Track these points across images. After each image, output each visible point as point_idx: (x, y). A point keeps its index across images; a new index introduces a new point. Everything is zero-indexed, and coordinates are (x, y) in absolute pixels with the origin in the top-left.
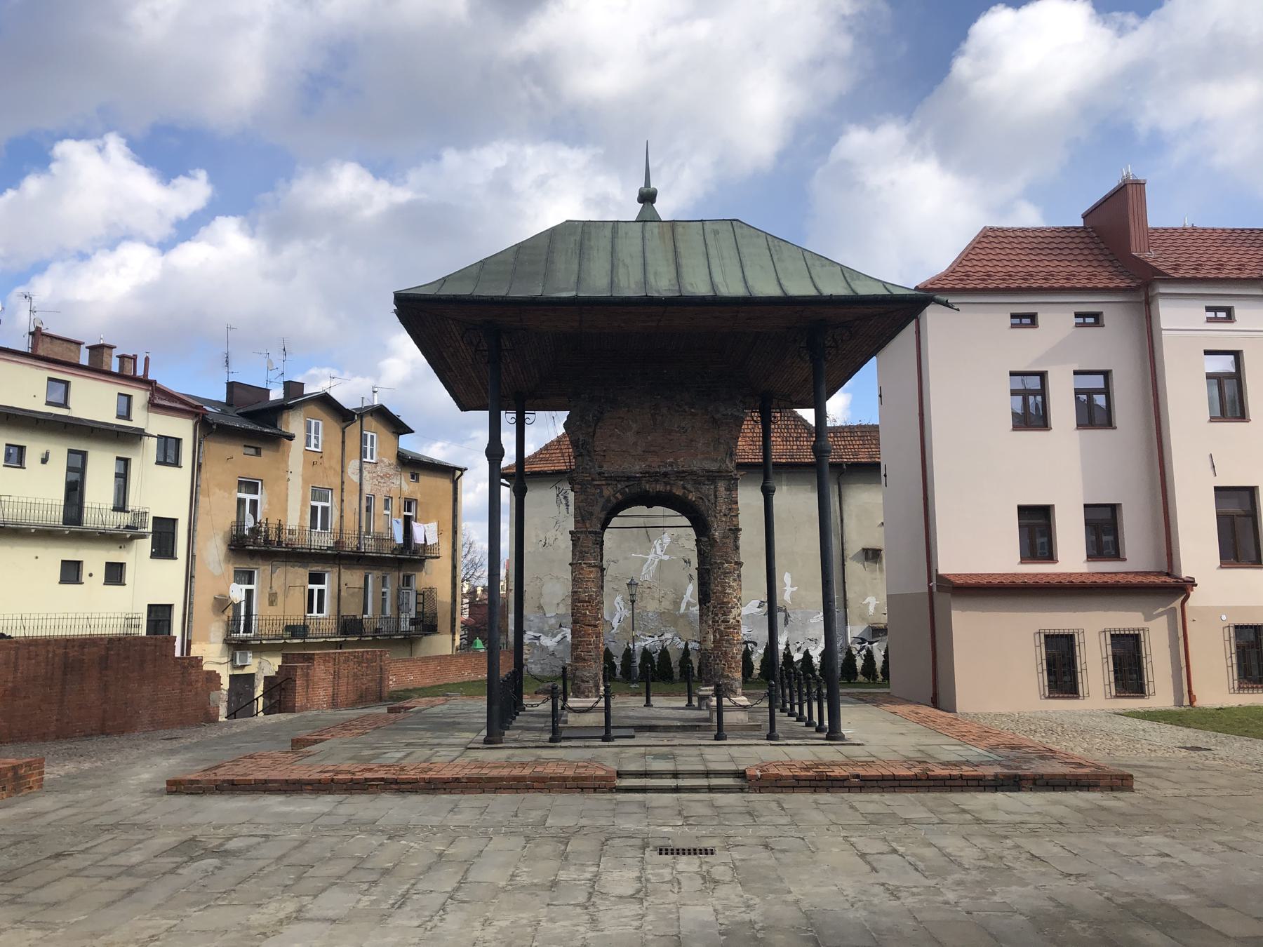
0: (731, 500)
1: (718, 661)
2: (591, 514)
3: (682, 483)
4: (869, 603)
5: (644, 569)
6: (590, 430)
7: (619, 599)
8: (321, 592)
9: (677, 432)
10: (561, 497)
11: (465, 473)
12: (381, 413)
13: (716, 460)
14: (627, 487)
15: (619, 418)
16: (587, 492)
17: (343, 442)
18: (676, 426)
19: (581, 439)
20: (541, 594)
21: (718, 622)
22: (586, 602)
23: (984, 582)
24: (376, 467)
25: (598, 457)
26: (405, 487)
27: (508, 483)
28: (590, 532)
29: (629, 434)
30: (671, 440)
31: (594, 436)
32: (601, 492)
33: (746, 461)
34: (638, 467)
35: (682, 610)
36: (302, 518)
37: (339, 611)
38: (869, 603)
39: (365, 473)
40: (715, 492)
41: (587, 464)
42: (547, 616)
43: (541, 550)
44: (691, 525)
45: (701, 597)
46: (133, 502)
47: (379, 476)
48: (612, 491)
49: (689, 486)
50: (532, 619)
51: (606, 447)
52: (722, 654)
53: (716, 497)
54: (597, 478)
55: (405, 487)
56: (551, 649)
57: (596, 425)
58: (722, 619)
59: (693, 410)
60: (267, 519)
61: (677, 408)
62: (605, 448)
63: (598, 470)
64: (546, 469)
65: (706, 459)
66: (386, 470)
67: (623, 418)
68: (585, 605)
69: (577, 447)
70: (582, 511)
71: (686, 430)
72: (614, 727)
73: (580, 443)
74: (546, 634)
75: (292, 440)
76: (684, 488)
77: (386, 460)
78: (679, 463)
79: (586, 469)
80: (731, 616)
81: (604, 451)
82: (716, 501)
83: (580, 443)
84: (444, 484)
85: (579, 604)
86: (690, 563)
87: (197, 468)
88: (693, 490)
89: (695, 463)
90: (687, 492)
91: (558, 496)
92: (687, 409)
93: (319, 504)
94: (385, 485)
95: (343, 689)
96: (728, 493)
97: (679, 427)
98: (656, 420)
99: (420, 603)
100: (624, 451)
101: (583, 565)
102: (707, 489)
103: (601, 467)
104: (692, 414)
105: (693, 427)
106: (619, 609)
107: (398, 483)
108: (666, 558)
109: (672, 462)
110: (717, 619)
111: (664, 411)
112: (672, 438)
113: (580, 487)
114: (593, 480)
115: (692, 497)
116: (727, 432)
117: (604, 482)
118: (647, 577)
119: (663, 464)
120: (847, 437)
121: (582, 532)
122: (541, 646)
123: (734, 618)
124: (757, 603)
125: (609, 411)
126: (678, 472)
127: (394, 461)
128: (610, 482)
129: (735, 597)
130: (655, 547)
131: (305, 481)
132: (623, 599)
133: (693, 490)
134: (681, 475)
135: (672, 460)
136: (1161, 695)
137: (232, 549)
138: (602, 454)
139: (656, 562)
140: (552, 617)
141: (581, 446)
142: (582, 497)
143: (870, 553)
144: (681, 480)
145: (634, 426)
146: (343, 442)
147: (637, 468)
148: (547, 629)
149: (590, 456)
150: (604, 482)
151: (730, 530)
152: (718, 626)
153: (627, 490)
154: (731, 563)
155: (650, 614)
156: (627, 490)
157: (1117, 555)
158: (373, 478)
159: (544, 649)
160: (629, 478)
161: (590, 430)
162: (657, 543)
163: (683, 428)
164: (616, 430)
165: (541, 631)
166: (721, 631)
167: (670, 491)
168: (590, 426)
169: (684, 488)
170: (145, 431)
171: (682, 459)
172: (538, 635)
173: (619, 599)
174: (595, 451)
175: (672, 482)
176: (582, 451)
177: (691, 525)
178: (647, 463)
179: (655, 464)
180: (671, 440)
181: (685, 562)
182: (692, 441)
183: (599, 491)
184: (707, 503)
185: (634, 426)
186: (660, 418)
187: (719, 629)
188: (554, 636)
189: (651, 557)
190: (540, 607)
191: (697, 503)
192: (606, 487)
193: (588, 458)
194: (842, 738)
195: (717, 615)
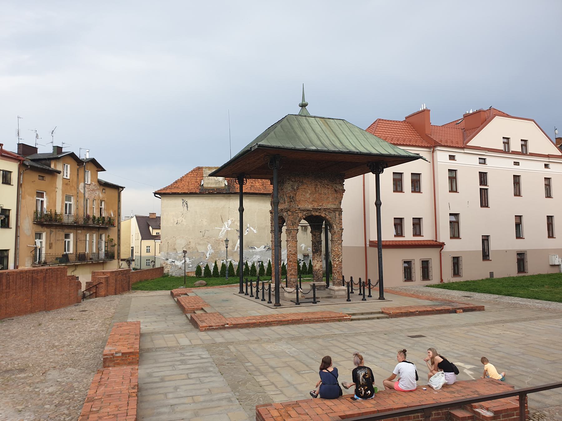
1: (336, 274)
2: (295, 223)
5: (220, 233)
6: (295, 193)
7: (209, 245)
10: (185, 204)
11: (124, 189)
12: (93, 161)
13: (335, 205)
15: (304, 188)
17: (78, 175)
20: (175, 244)
22: (294, 254)
23: (391, 243)
24: (90, 186)
26: (101, 195)
27: (160, 197)
28: (295, 230)
29: (307, 194)
33: (261, 192)
34: (310, 206)
35: (235, 250)
36: (62, 209)
37: (76, 251)
39: (86, 189)
42: (178, 252)
43: (175, 225)
45: (314, 251)
49: (327, 214)
50: (171, 254)
53: (335, 218)
55: (101, 195)
56: (180, 266)
60: (51, 210)
64: (178, 191)
65: (333, 204)
66: (93, 187)
72: (312, 298)
73: (291, 197)
74: (177, 260)
75: (60, 174)
76: (325, 214)
77: (93, 183)
80: (340, 259)
83: (291, 197)
84: (114, 193)
87: (19, 185)
91: (183, 203)
93: (68, 203)
95: (118, 286)
102: (332, 214)
103: (298, 206)
104: (328, 188)
105: (328, 193)
106: (209, 250)
107: (98, 193)
108: (229, 229)
110: (335, 260)
111: (319, 186)
114: (296, 211)
115: (327, 217)
118: (221, 237)
122: (175, 265)
124: (264, 246)
127: (97, 184)
130: (225, 225)
131: (63, 192)
132: (211, 245)
134: (325, 210)
135: (321, 204)
136: (435, 279)
137: (35, 224)
139: (225, 231)
140: (180, 253)
142: (292, 217)
143: (303, 228)
147: (310, 207)
148: (178, 258)
154: (340, 240)
155: (222, 252)
157: (420, 235)
158: (89, 191)
159: (176, 266)
160: (308, 210)
162: (226, 223)
165: (175, 259)
167: (321, 215)
169: (325, 214)
172: (174, 261)
173: (209, 245)
179: (316, 206)
182: (328, 198)
188: (181, 261)
189: (223, 229)
190: (175, 249)
194: (384, 299)
195: (335, 258)
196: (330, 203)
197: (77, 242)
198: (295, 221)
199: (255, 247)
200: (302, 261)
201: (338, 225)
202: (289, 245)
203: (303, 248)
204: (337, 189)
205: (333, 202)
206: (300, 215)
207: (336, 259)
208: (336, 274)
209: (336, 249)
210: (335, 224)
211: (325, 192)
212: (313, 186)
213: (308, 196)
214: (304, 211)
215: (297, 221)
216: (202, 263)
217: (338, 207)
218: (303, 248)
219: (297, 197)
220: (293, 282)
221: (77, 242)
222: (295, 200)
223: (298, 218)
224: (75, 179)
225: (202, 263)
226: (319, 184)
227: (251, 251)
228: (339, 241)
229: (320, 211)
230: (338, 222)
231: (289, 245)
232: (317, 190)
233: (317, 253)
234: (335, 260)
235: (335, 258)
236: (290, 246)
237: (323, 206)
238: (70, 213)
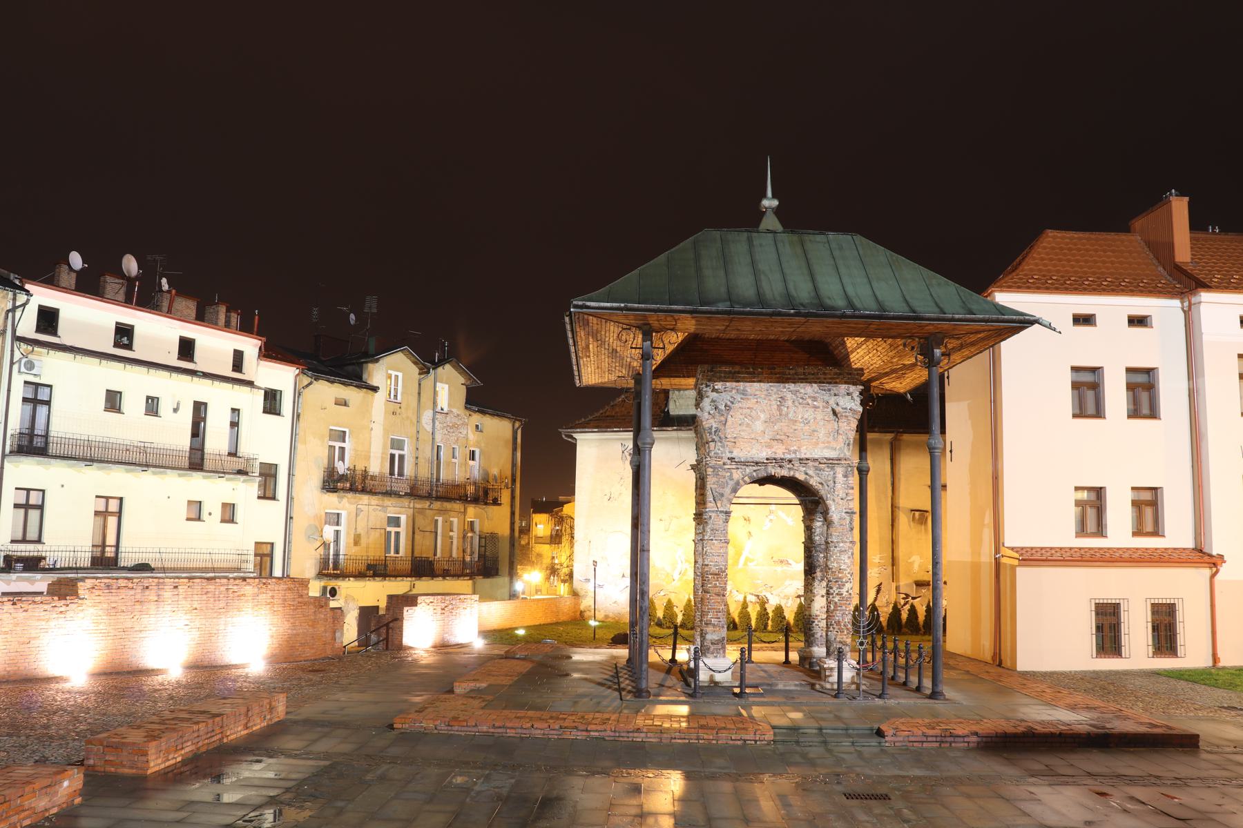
0: (848, 486)
2: (722, 495)
3: (804, 469)
4: (914, 561)
8: (397, 534)
9: (800, 423)
13: (835, 449)
14: (755, 471)
16: (719, 475)
17: (419, 394)
18: (800, 417)
21: (832, 594)
22: (716, 574)
25: (728, 443)
28: (721, 512)
29: (757, 423)
30: (795, 430)
31: (725, 424)
32: (731, 473)
38: (914, 561)
39: (437, 423)
40: (835, 478)
41: (719, 449)
44: (798, 503)
45: (807, 568)
46: (244, 450)
47: (448, 426)
48: (741, 475)
49: (810, 472)
52: (835, 622)
54: (729, 462)
57: (728, 414)
58: (837, 592)
59: (815, 403)
60: (355, 466)
61: (801, 401)
62: (735, 436)
63: (729, 455)
66: (455, 420)
67: (752, 408)
68: (715, 577)
70: (714, 492)
71: (809, 421)
73: (714, 430)
75: (377, 392)
76: (807, 474)
78: (802, 451)
79: (718, 454)
81: (735, 438)
82: (834, 486)
83: (714, 430)
85: (710, 577)
86: (749, 520)
87: (297, 417)
88: (814, 475)
89: (816, 451)
90: (808, 477)
91: (623, 452)
92: (810, 402)
93: (397, 453)
94: (454, 434)
96: (845, 479)
97: (801, 419)
98: (782, 410)
99: (482, 547)
100: (752, 439)
101: (714, 541)
104: (816, 407)
105: (815, 418)
107: (465, 432)
109: (796, 451)
112: (796, 427)
113: (712, 470)
114: (724, 464)
116: (845, 424)
117: (734, 467)
119: (787, 451)
121: (713, 511)
123: (847, 592)
125: (739, 402)
126: (800, 459)
128: (739, 466)
129: (849, 573)
133: (814, 475)
135: (795, 448)
138: (733, 441)
141: (713, 433)
144: (804, 467)
145: (762, 416)
146: (419, 394)
147: (762, 454)
149: (721, 442)
150: (734, 467)
151: (846, 513)
152: (833, 597)
153: (755, 474)
154: (846, 542)
156: (755, 474)
157: (1157, 532)
161: (723, 419)
163: (806, 419)
164: (746, 419)
166: (836, 603)
168: (723, 415)
169: (807, 474)
170: (255, 383)
171: (805, 447)
174: (726, 438)
175: (795, 468)
176: (714, 437)
177: (798, 503)
178: (773, 450)
179: (780, 451)
180: (795, 430)
181: (745, 519)
182: (814, 431)
183: (729, 474)
184: (826, 487)
185: (762, 416)
186: (786, 409)
187: (833, 601)
191: (816, 487)
192: (735, 470)
193: (719, 444)
195: (831, 588)
196: (821, 445)
197: (414, 533)
198: (721, 491)
199: (790, 561)
201: (841, 502)
203: (916, 566)
204: (838, 409)
205: (828, 442)
206: (737, 475)
207: (835, 589)
208: (831, 629)
210: (834, 500)
211: (806, 416)
212: (774, 402)
213: (759, 426)
214: (746, 463)
215: (727, 490)
216: (662, 593)
217: (842, 456)
218: (916, 566)
219: (728, 431)
220: (712, 643)
221: (414, 533)
222: (722, 436)
223: (731, 483)
224: (414, 403)
225: (662, 593)
226: (789, 396)
227: (779, 568)
228: (841, 545)
229: (790, 466)
230: (842, 494)
232: (784, 413)
237: (800, 453)
238: (401, 474)
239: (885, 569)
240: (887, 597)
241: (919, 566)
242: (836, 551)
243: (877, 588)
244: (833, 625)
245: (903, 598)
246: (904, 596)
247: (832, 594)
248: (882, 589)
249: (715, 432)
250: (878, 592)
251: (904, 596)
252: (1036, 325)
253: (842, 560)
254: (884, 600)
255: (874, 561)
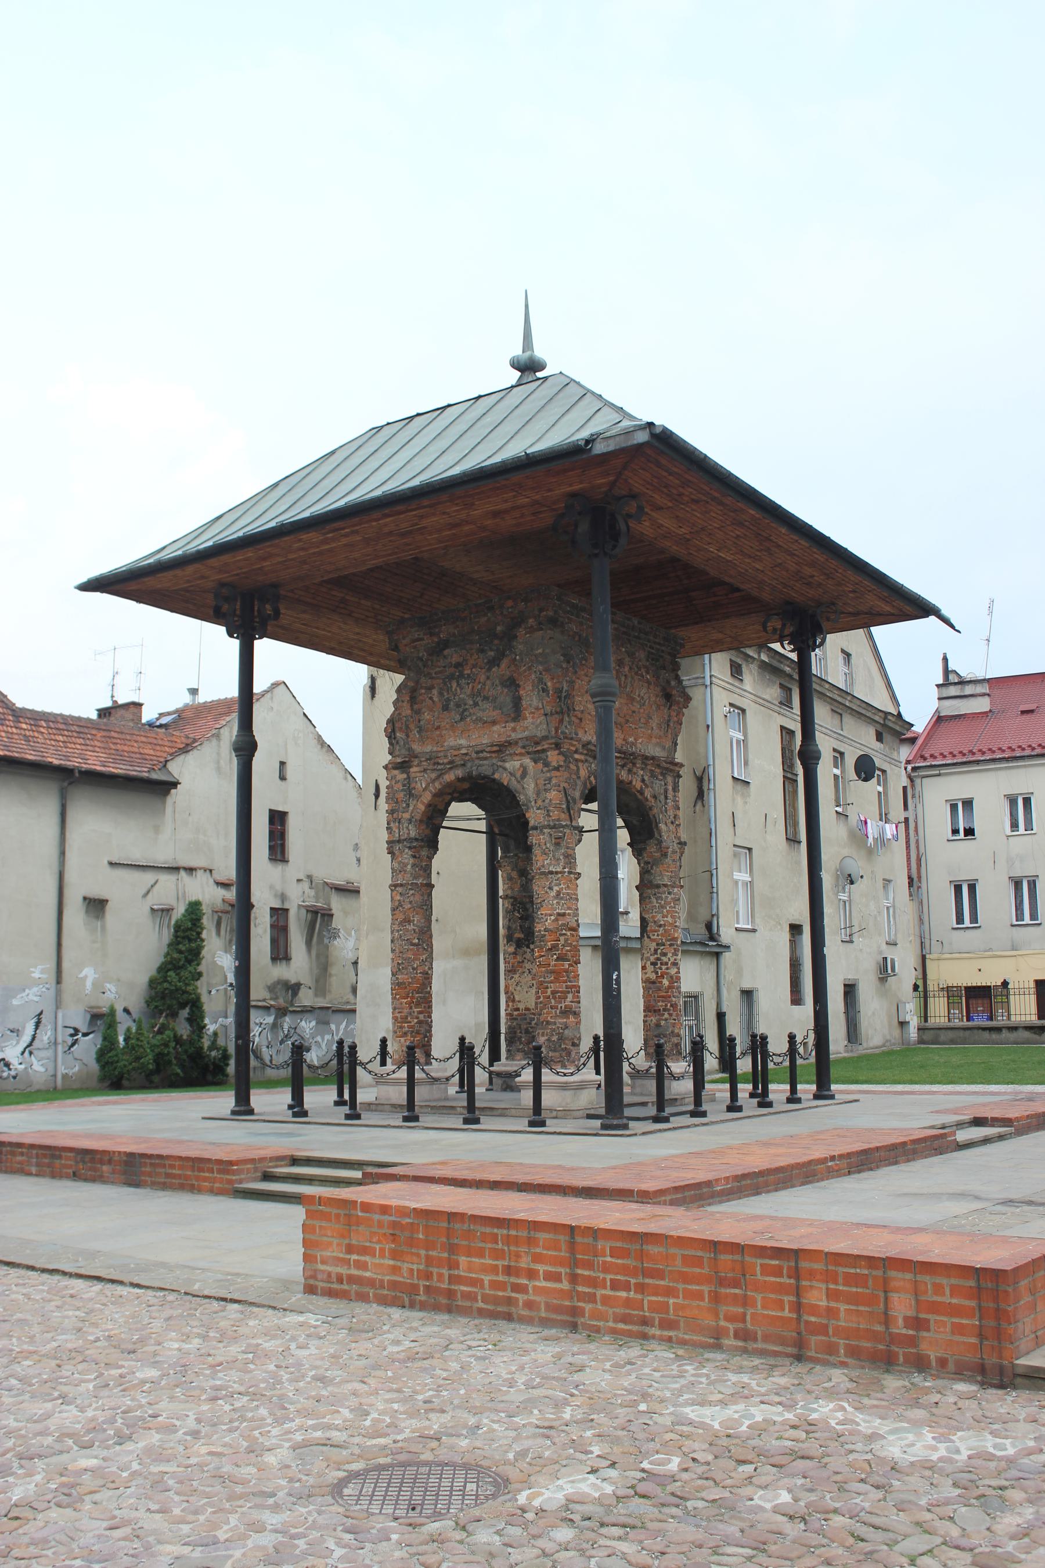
1: (666, 1016)
4: (86, 976)
19: (565, 688)
21: (666, 964)
38: (86, 976)
51: (584, 706)
53: (666, 798)
58: (672, 960)
69: (560, 697)
73: (564, 694)
83: (564, 694)
97: (639, 696)
110: (665, 959)
114: (576, 752)
120: (63, 730)
135: (631, 739)
152: (667, 969)
166: (671, 977)
174: (574, 710)
187: (667, 974)
196: (654, 740)
200: (85, 1035)
202: (556, 888)
203: (89, 984)
207: (670, 955)
208: (666, 1016)
209: (670, 919)
231: (556, 888)
233: (532, 946)
234: (665, 959)
235: (665, 955)
236: (558, 893)
239: (48, 989)
240: (49, 1033)
241: (93, 984)
242: (669, 900)
243: (35, 1020)
244: (669, 1010)
245: (72, 1035)
246: (72, 1031)
247: (666, 964)
248: (44, 1021)
249: (565, 697)
250: (38, 1025)
251: (72, 1031)
252: (932, 618)
253: (676, 912)
254: (45, 1038)
255: (33, 975)
